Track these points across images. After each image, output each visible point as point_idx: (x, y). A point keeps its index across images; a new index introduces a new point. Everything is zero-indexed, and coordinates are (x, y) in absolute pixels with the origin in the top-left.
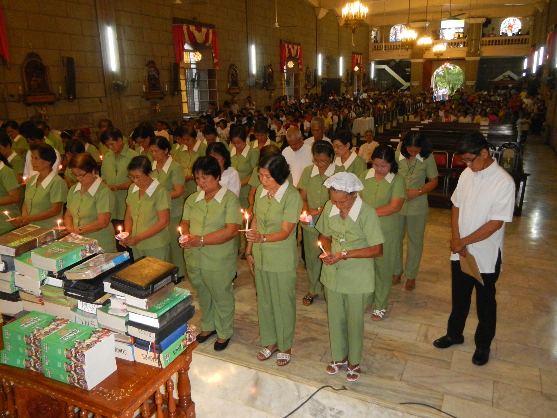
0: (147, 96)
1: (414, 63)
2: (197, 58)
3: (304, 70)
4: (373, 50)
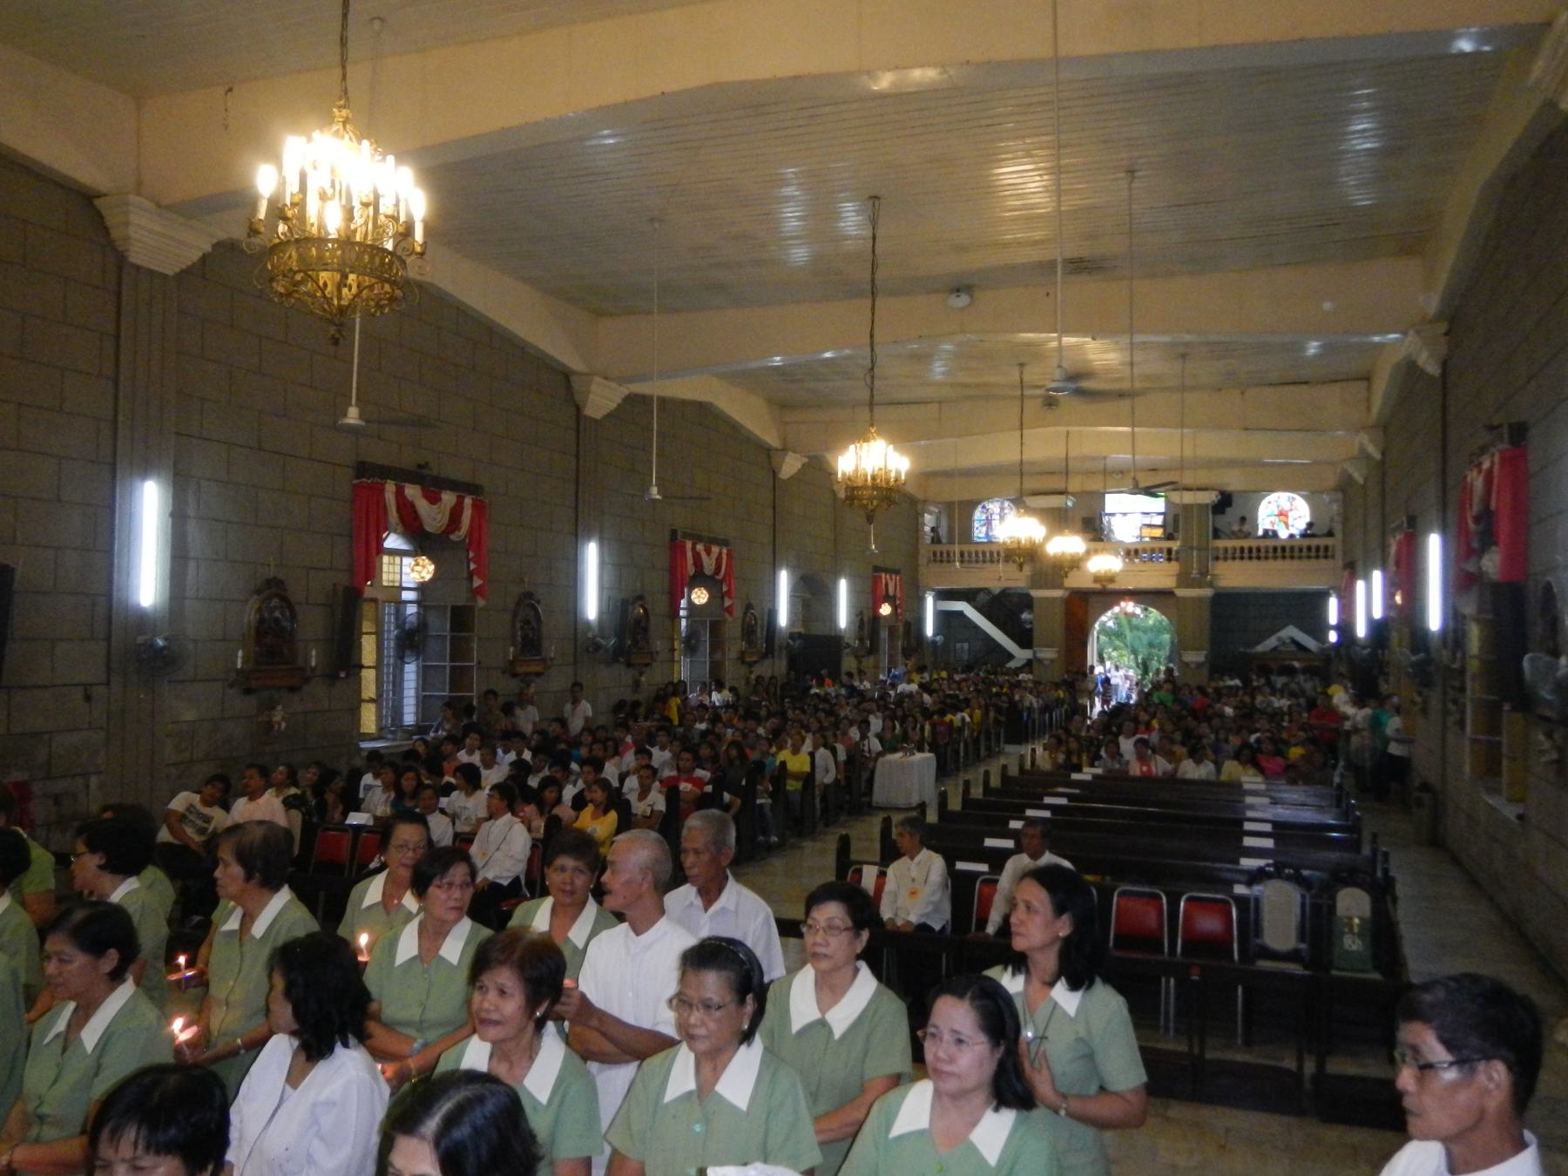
0: (246, 683)
2: (420, 572)
3: (738, 613)
4: (929, 562)
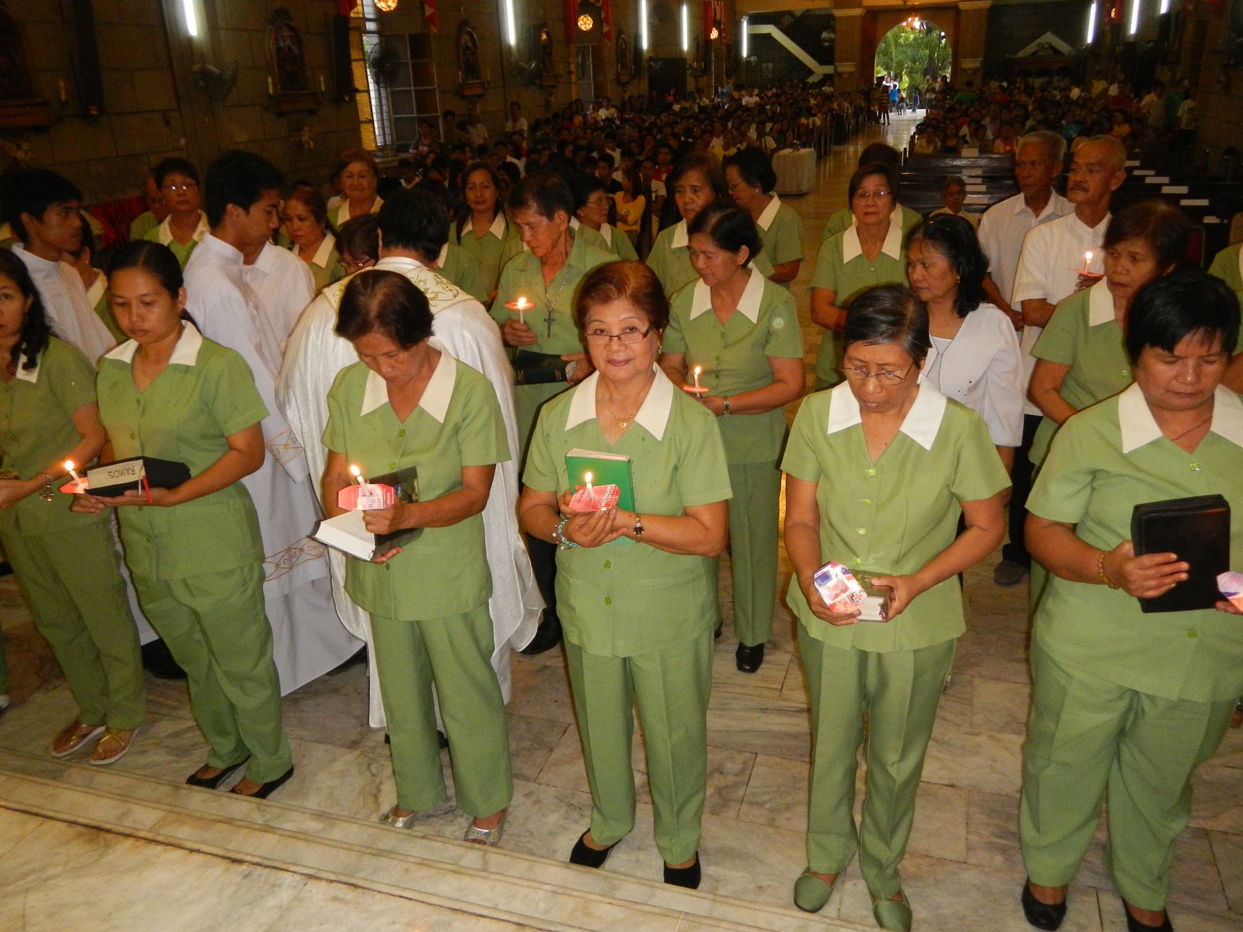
1: (842, 17)
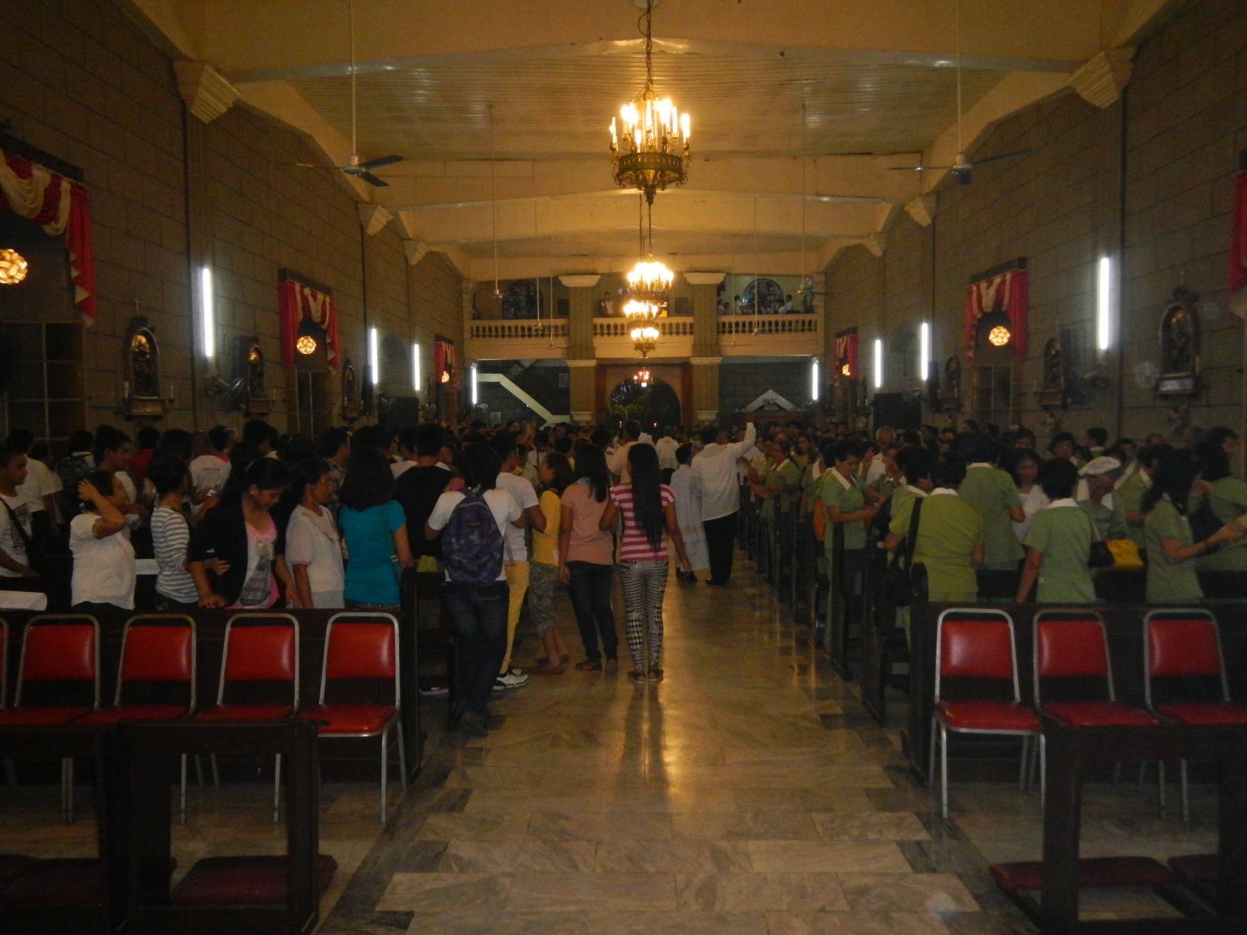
1: (576, 368)
